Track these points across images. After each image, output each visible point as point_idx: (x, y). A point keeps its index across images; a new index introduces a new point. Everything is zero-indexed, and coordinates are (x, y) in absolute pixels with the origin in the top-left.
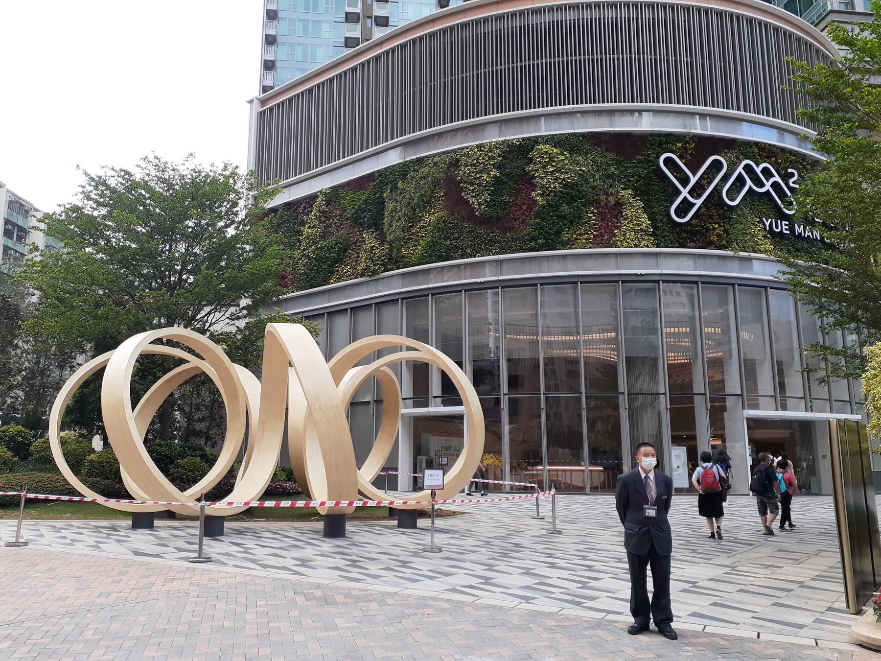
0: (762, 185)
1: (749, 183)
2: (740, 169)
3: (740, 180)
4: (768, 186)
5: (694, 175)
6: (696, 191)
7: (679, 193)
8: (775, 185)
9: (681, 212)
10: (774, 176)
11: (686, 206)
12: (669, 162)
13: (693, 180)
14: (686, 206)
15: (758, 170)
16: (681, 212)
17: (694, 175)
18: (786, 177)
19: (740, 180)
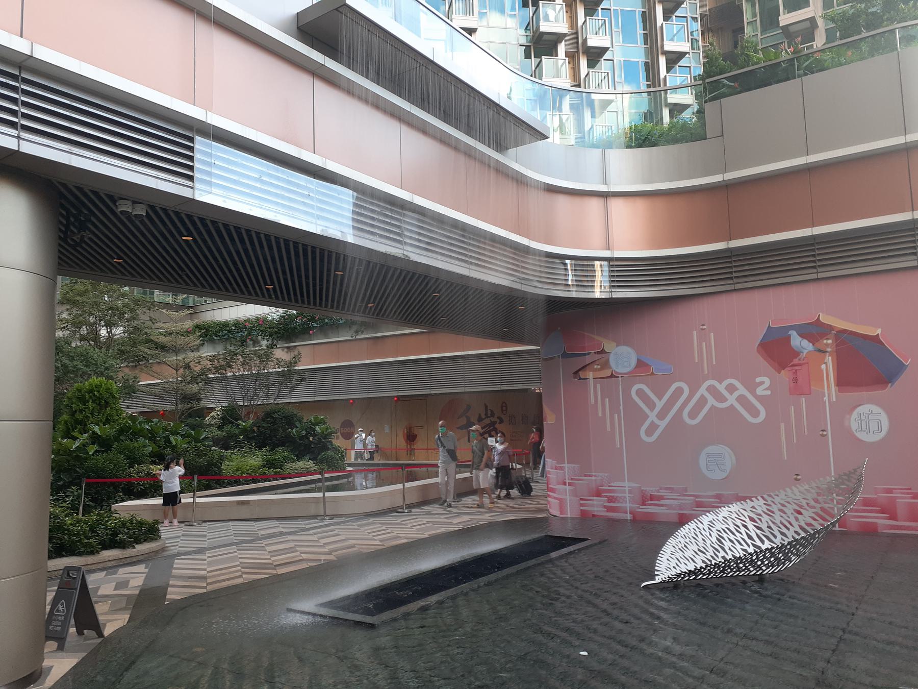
0: (725, 400)
1: (711, 401)
2: (702, 390)
3: (703, 401)
5: (660, 398)
6: (661, 416)
7: (647, 417)
8: (741, 399)
9: (649, 433)
10: (737, 389)
11: (653, 427)
13: (660, 404)
14: (653, 427)
15: (721, 387)
16: (649, 433)
17: (660, 398)
18: (752, 387)
19: (703, 401)
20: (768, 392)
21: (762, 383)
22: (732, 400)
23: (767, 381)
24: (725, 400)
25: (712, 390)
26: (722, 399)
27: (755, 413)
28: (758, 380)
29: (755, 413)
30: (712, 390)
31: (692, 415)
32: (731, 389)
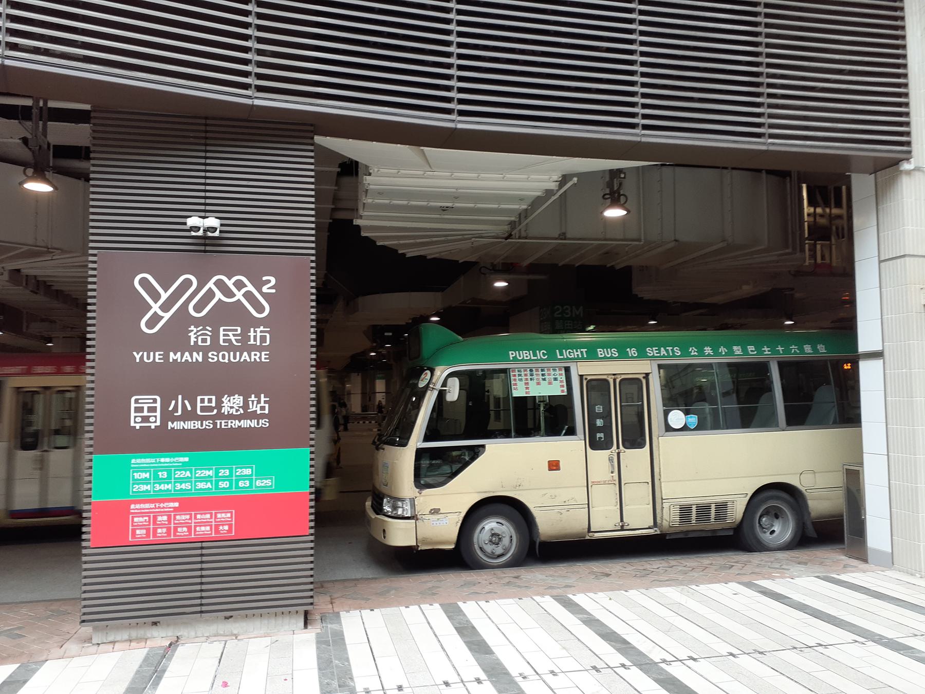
0: (234, 295)
1: (219, 295)
2: (211, 285)
4: (239, 295)
6: (165, 307)
8: (248, 296)
9: (151, 324)
11: (156, 318)
12: (144, 282)
13: (164, 296)
14: (156, 318)
15: (230, 283)
18: (258, 285)
19: (210, 294)
20: (273, 291)
21: (269, 281)
22: (239, 295)
23: (273, 281)
24: (234, 295)
25: (220, 285)
26: (230, 294)
27: (260, 309)
28: (264, 278)
29: (260, 309)
30: (220, 285)
31: (198, 308)
32: (239, 285)
